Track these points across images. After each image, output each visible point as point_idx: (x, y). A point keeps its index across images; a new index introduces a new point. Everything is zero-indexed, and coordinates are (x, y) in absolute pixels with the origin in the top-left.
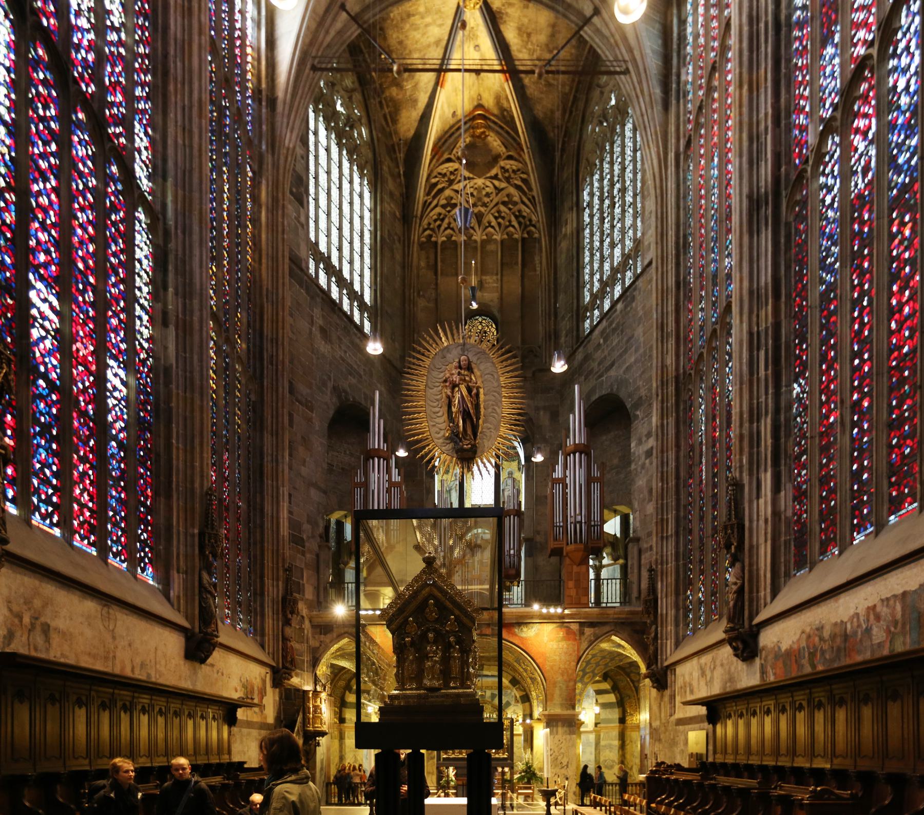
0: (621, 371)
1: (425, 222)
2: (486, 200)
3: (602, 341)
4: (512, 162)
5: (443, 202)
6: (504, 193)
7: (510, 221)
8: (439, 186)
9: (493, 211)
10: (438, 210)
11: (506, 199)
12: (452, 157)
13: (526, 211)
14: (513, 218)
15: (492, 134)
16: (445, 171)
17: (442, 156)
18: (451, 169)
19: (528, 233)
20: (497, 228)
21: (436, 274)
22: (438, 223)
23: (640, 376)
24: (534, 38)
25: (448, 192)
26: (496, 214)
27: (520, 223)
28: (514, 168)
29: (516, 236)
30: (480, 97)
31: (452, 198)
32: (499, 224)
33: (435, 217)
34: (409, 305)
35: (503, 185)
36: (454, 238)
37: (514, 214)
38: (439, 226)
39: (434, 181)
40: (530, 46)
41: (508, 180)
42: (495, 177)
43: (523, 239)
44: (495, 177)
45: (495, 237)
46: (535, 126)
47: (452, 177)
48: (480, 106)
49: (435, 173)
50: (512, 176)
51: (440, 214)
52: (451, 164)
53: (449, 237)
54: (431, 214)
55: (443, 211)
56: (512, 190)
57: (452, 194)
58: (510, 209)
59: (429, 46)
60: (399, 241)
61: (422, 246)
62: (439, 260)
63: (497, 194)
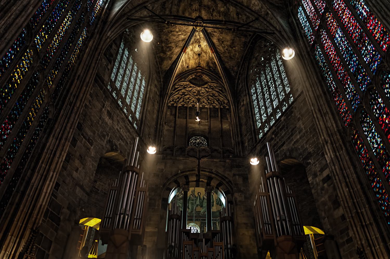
0: (291, 145)
1: (171, 99)
2: (202, 94)
3: (273, 136)
4: (214, 84)
5: (181, 94)
6: (211, 92)
7: (214, 102)
8: (179, 89)
9: (205, 98)
10: (178, 96)
11: (212, 95)
12: (186, 80)
13: (221, 99)
14: (215, 101)
15: (204, 75)
16: (182, 84)
17: (181, 79)
18: (185, 84)
19: (223, 106)
20: (208, 104)
21: (175, 118)
22: (178, 100)
23: (306, 143)
24: (225, 43)
25: (183, 91)
26: (207, 99)
27: (219, 103)
28: (215, 86)
29: (217, 107)
30: (199, 63)
31: (185, 93)
32: (209, 103)
33: (176, 98)
34: (160, 126)
35: (210, 90)
36: (185, 105)
37: (216, 99)
38: (178, 101)
39: (176, 87)
40: (223, 45)
41: (213, 89)
42: (207, 88)
43: (221, 109)
44: (207, 88)
45: (206, 106)
46: (225, 69)
47: (186, 86)
48: (199, 66)
49: (177, 84)
50: (214, 88)
51: (178, 97)
52: (185, 82)
53: (183, 105)
54: (174, 97)
55: (181, 96)
56: (214, 92)
57: (185, 91)
58: (214, 98)
59: (179, 41)
60: (158, 102)
61: (169, 107)
62: (177, 112)
63: (207, 93)
